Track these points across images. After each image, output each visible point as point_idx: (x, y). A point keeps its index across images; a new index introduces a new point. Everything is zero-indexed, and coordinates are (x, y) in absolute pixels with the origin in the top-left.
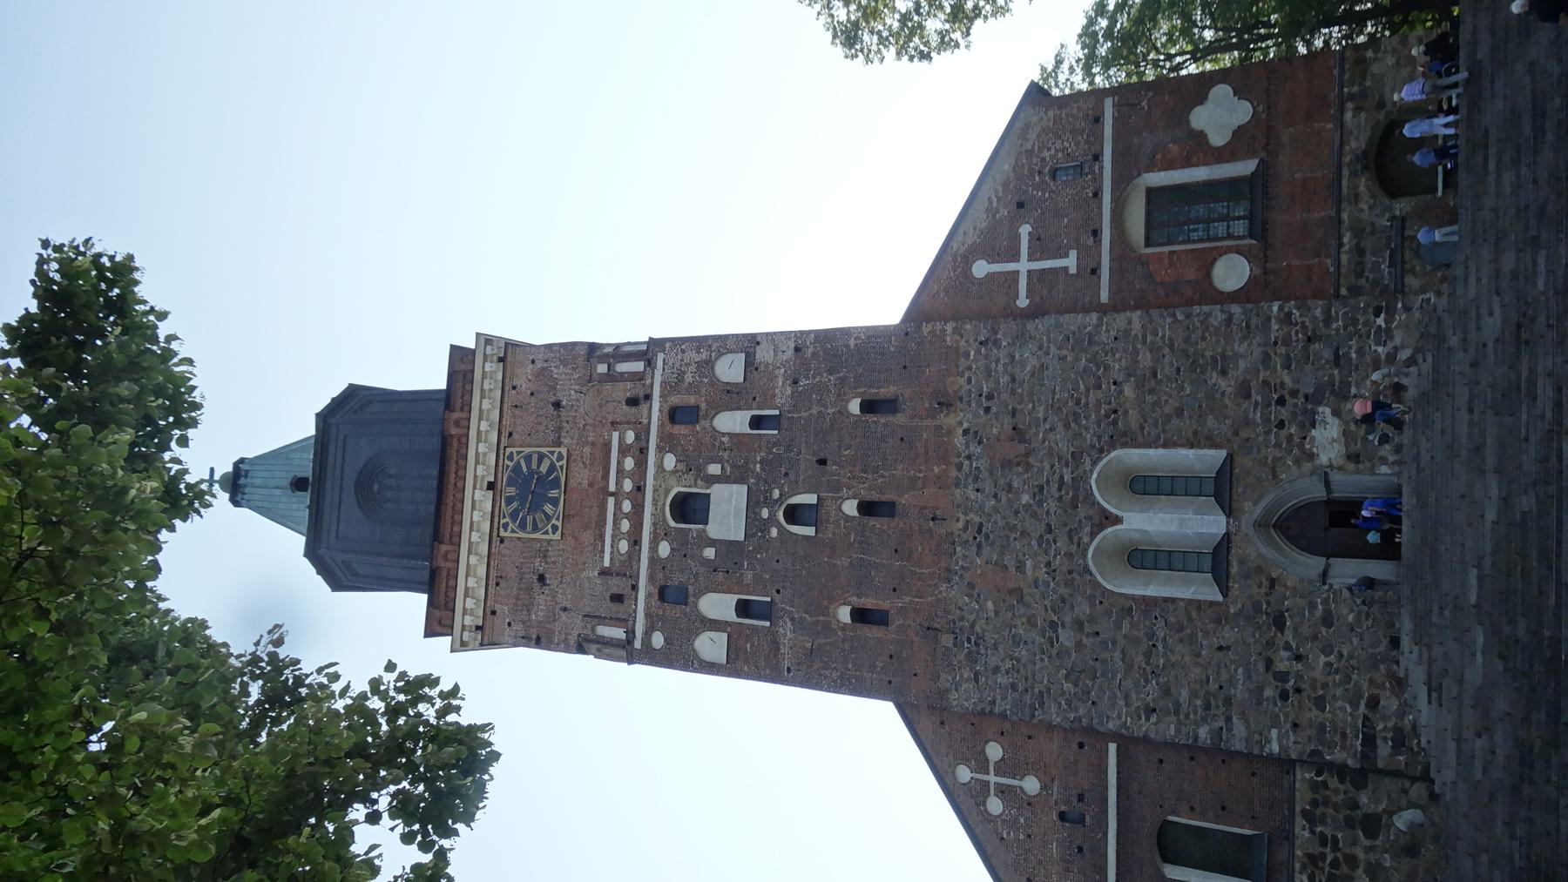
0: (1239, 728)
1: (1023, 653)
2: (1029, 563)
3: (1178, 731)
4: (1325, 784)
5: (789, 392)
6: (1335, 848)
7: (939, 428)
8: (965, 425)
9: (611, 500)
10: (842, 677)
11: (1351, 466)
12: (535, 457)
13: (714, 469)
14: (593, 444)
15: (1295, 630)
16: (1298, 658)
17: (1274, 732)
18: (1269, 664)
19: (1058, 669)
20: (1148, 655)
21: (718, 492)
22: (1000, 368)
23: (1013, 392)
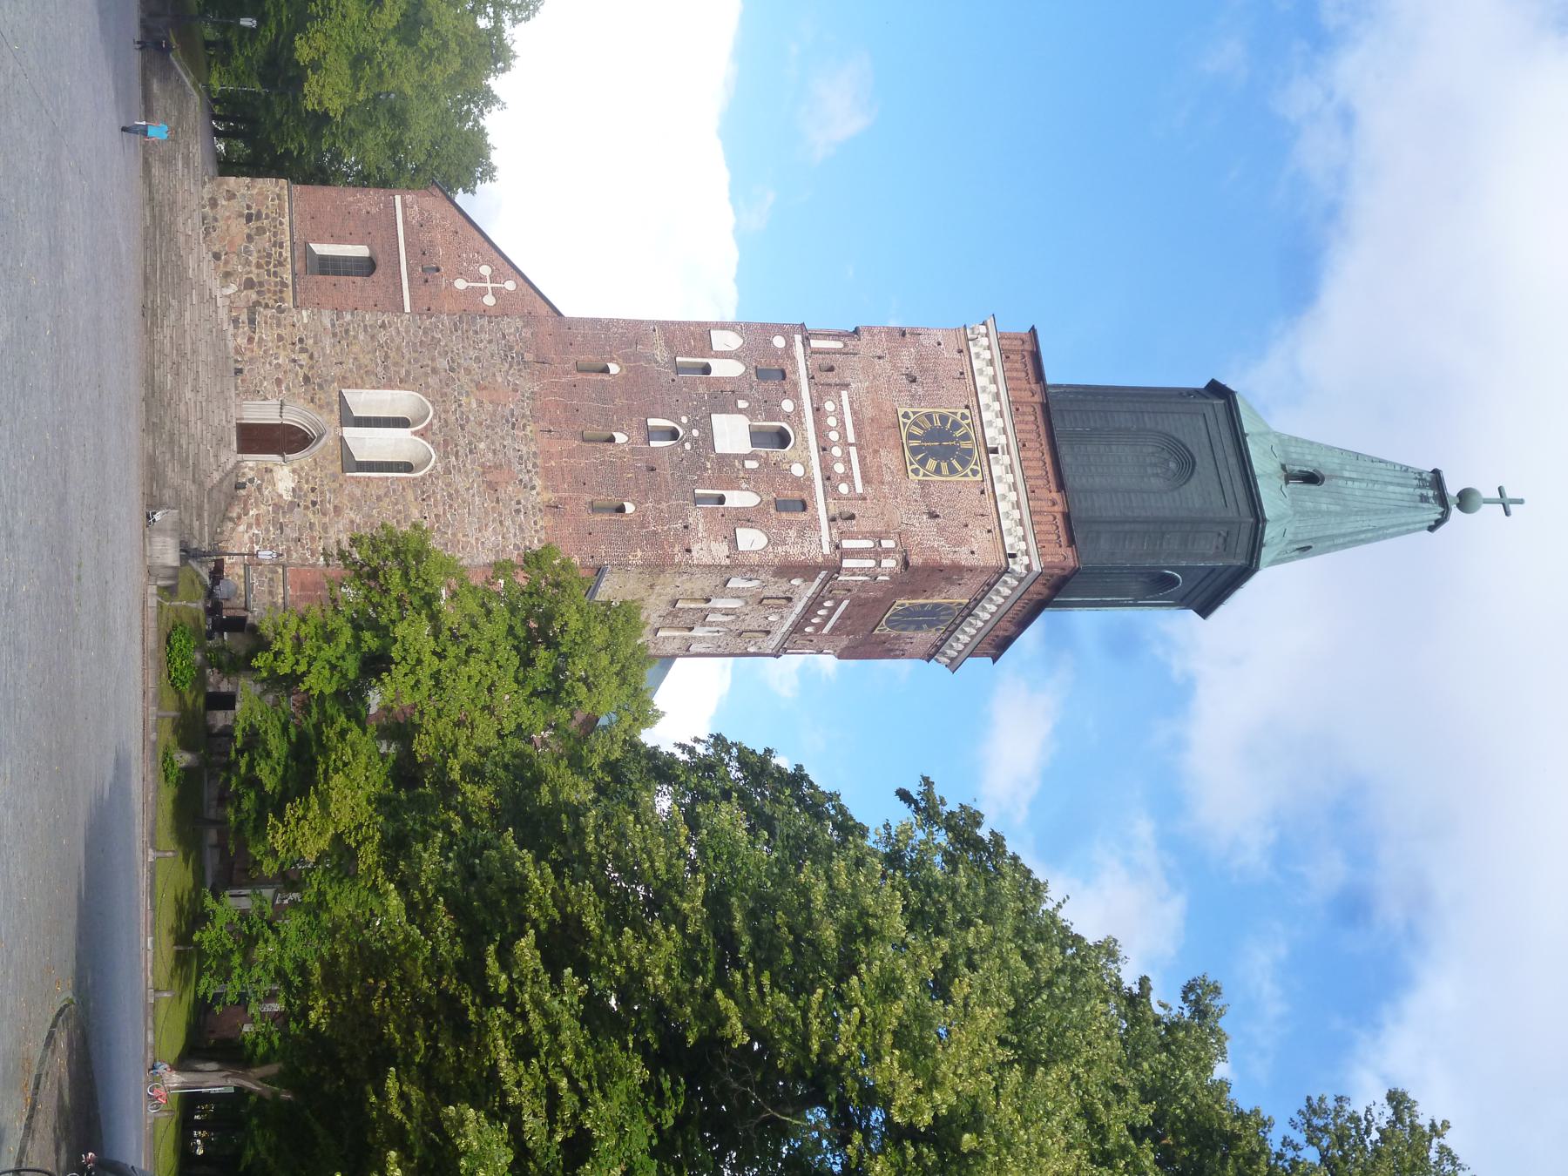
0: (327, 323)
1: (473, 354)
7: (555, 490)
13: (751, 464)
18: (311, 357)
20: (387, 356)
21: (745, 447)
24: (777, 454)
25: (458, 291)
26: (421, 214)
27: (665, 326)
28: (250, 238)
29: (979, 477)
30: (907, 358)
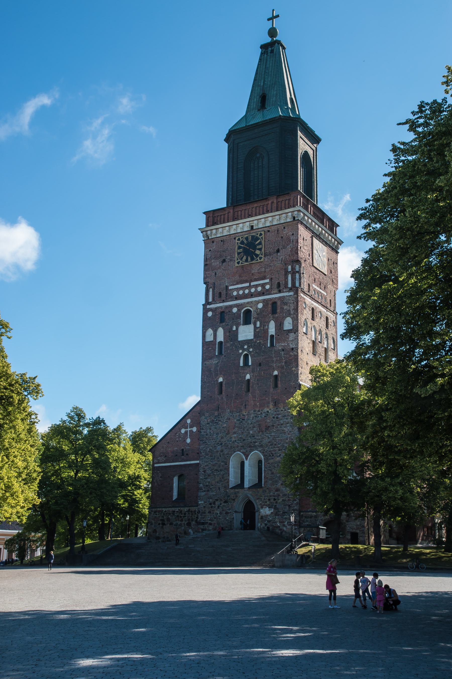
0: (203, 494)
2: (235, 435)
3: (201, 479)
4: (195, 514)
5: (280, 348)
6: (184, 517)
7: (269, 403)
8: (270, 411)
9: (247, 284)
10: (205, 382)
11: (260, 517)
12: (260, 247)
13: (258, 324)
14: (265, 271)
15: (224, 506)
16: (218, 507)
17: (203, 502)
18: (217, 500)
19: (212, 446)
20: (216, 470)
22: (285, 420)
23: (279, 425)
24: (254, 315)
25: (191, 442)
26: (161, 456)
27: (204, 360)
28: (171, 524)
29: (263, 233)
30: (216, 263)
